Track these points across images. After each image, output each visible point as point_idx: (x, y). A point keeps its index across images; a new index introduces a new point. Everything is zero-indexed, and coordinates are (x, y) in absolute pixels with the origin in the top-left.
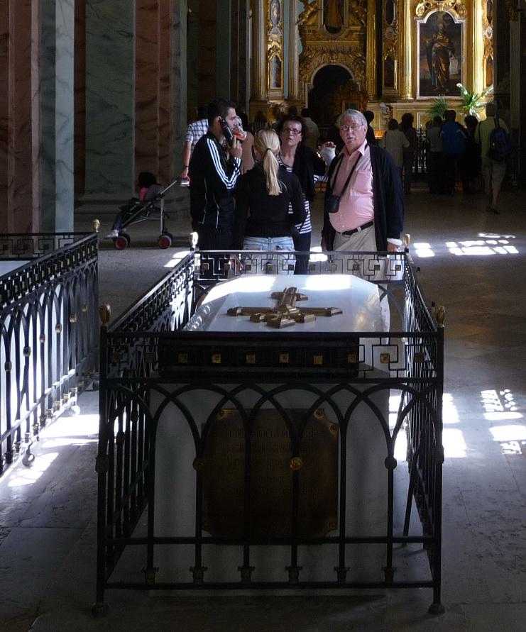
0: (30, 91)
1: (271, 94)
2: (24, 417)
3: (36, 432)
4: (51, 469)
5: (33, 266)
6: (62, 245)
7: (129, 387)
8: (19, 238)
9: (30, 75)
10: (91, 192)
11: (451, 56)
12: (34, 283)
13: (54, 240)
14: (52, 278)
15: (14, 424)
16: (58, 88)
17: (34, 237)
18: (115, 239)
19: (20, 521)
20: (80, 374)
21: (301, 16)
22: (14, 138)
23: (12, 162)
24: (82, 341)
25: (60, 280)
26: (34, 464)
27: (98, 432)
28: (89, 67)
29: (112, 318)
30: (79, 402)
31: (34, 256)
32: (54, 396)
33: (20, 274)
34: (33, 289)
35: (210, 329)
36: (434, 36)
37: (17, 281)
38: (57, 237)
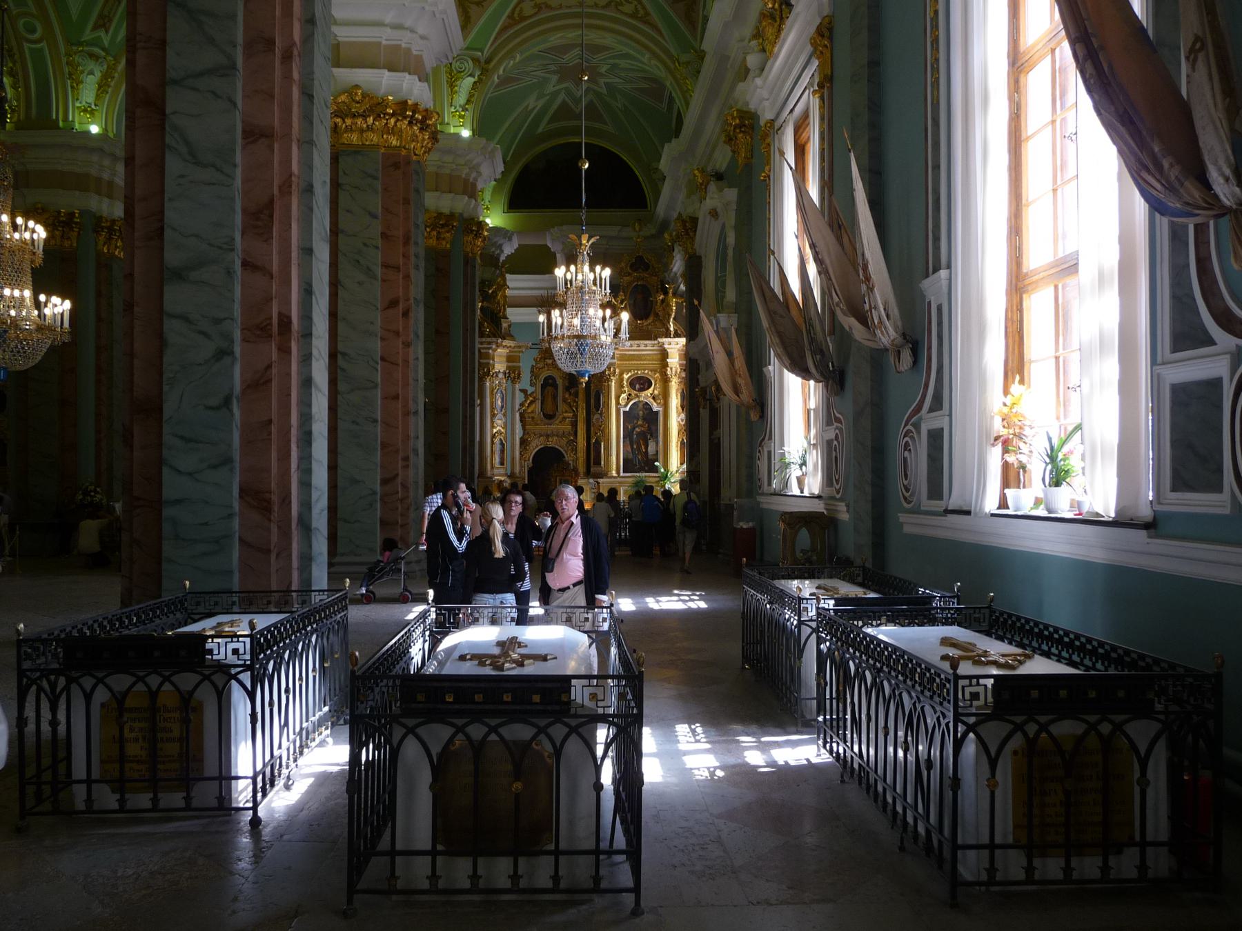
0: (290, 468)
1: (496, 471)
2: (285, 745)
3: (295, 760)
4: (307, 792)
5: (293, 619)
6: (317, 601)
7: (374, 721)
8: (281, 594)
9: (290, 455)
10: (343, 555)
12: (294, 633)
13: (310, 595)
14: (309, 628)
15: (276, 753)
16: (314, 466)
17: (293, 594)
18: (362, 595)
19: (282, 836)
20: (332, 710)
21: (522, 405)
22: (276, 509)
23: (274, 529)
24: (335, 680)
25: (316, 630)
26: (293, 787)
27: (348, 760)
28: (340, 448)
29: (361, 662)
30: (332, 735)
31: (294, 610)
32: (310, 729)
33: (281, 625)
34: (293, 638)
35: (444, 672)
37: (279, 631)
38: (313, 594)
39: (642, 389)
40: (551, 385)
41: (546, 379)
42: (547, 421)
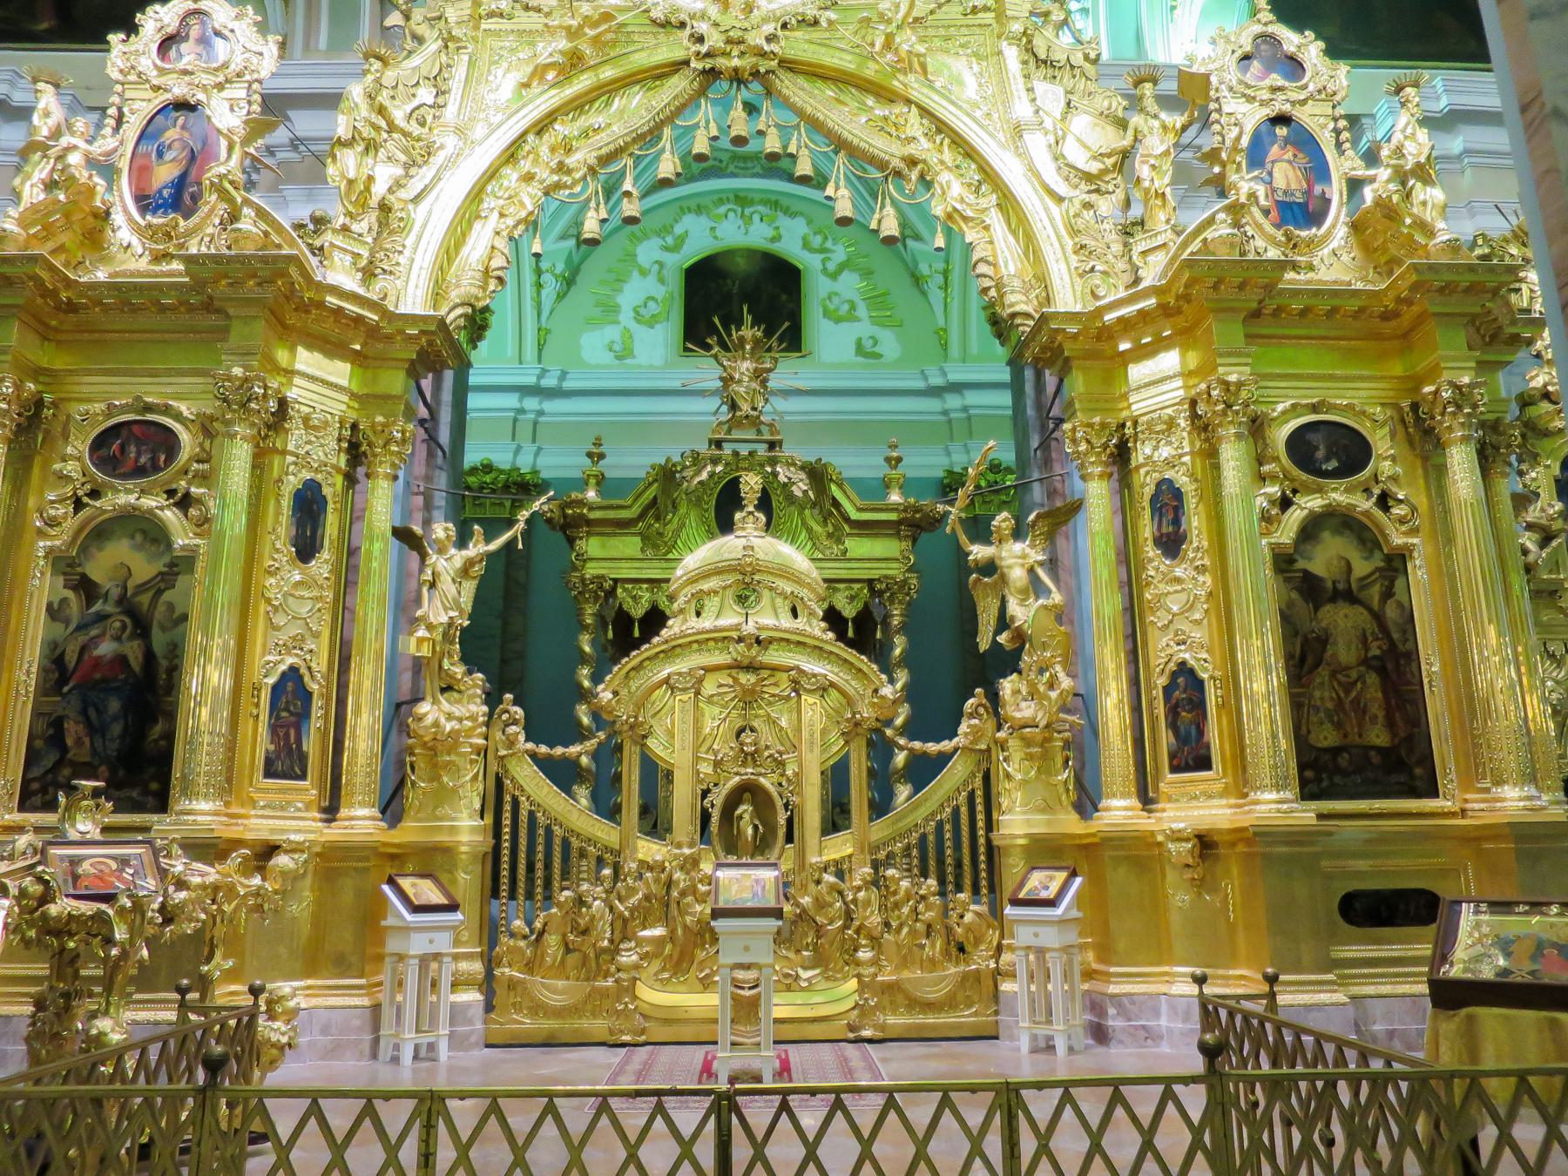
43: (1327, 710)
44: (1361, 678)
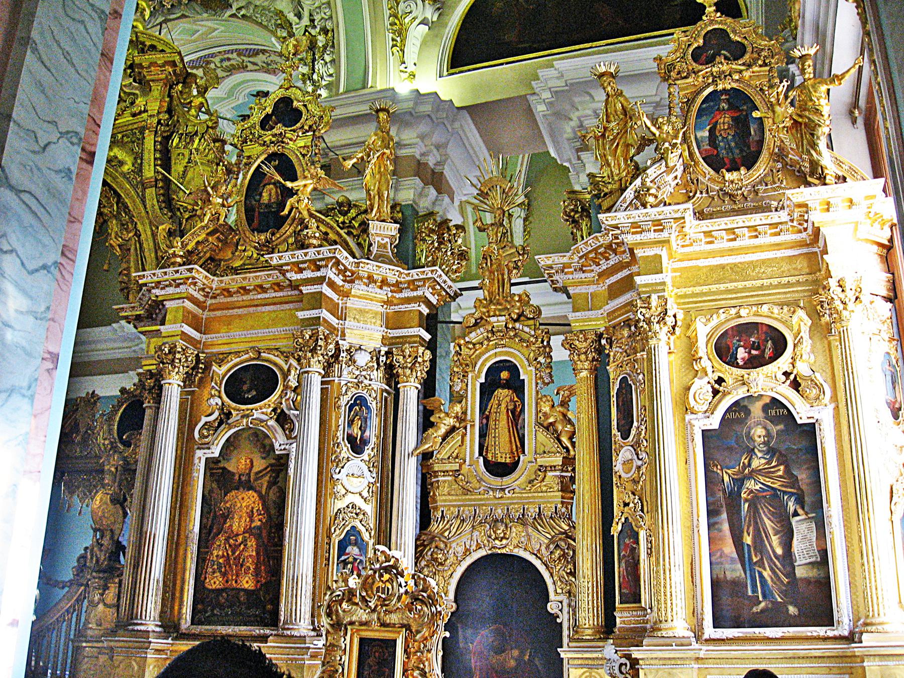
11: (796, 514)
36: (744, 460)
39: (754, 363)
40: (507, 385)
41: (494, 370)
42: (496, 481)
43: (219, 564)
44: (244, 541)
